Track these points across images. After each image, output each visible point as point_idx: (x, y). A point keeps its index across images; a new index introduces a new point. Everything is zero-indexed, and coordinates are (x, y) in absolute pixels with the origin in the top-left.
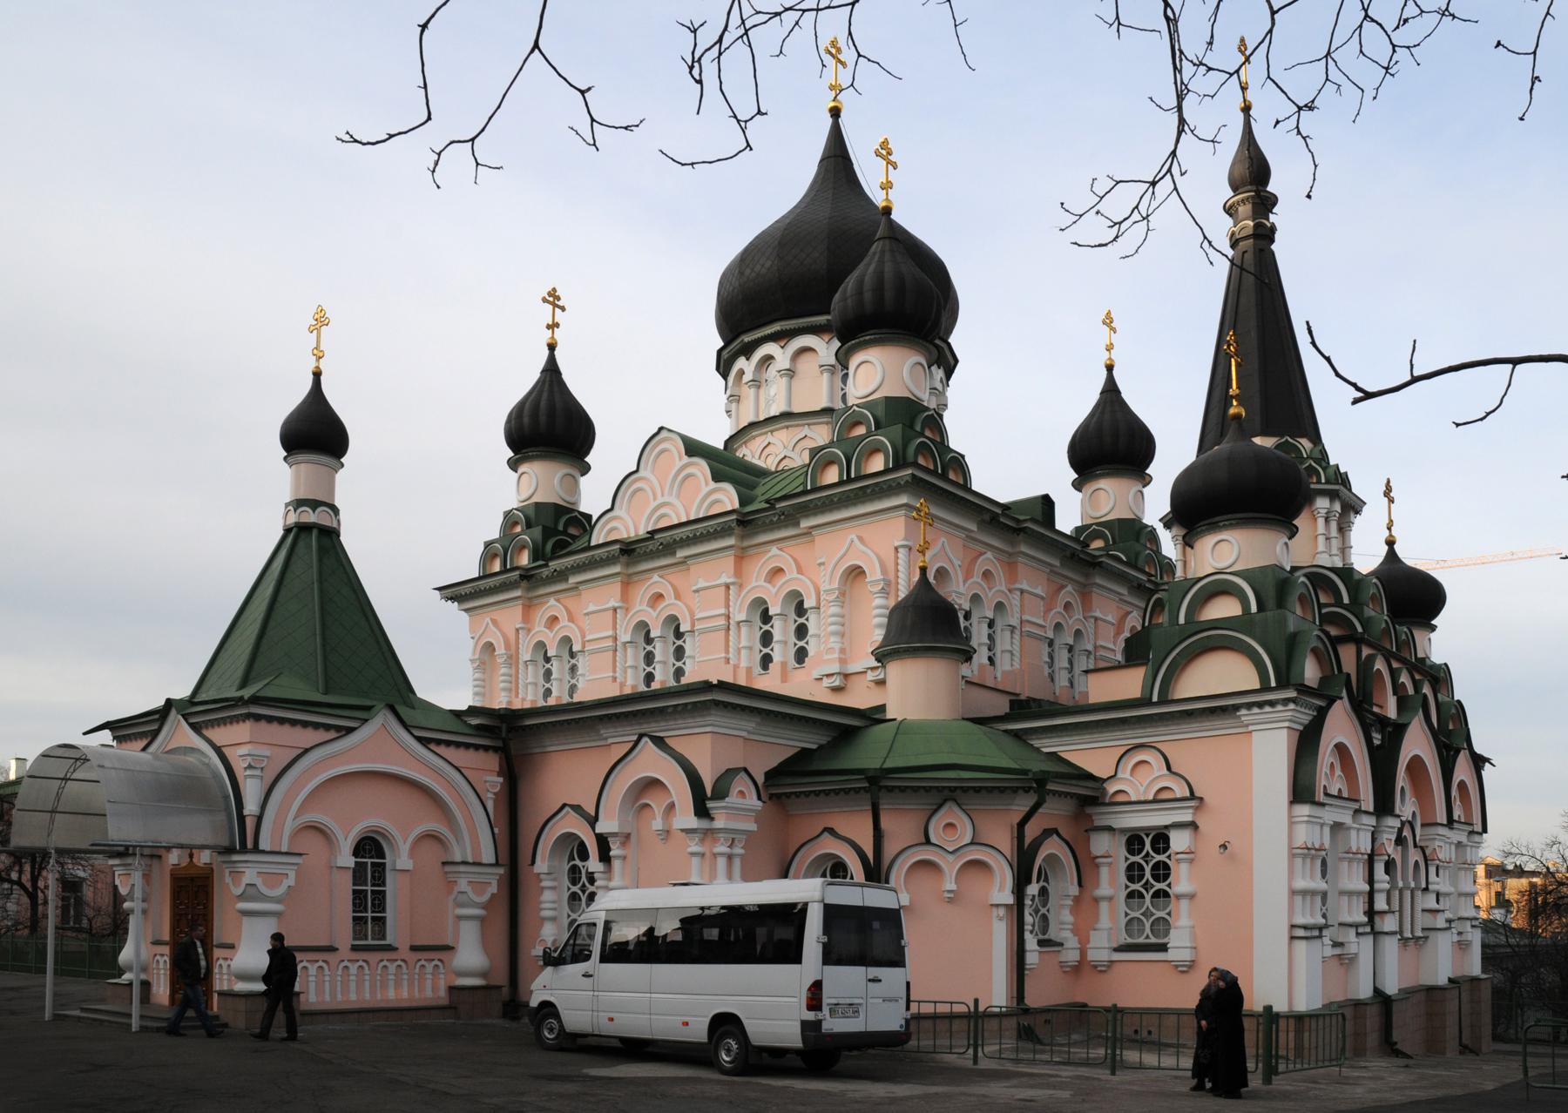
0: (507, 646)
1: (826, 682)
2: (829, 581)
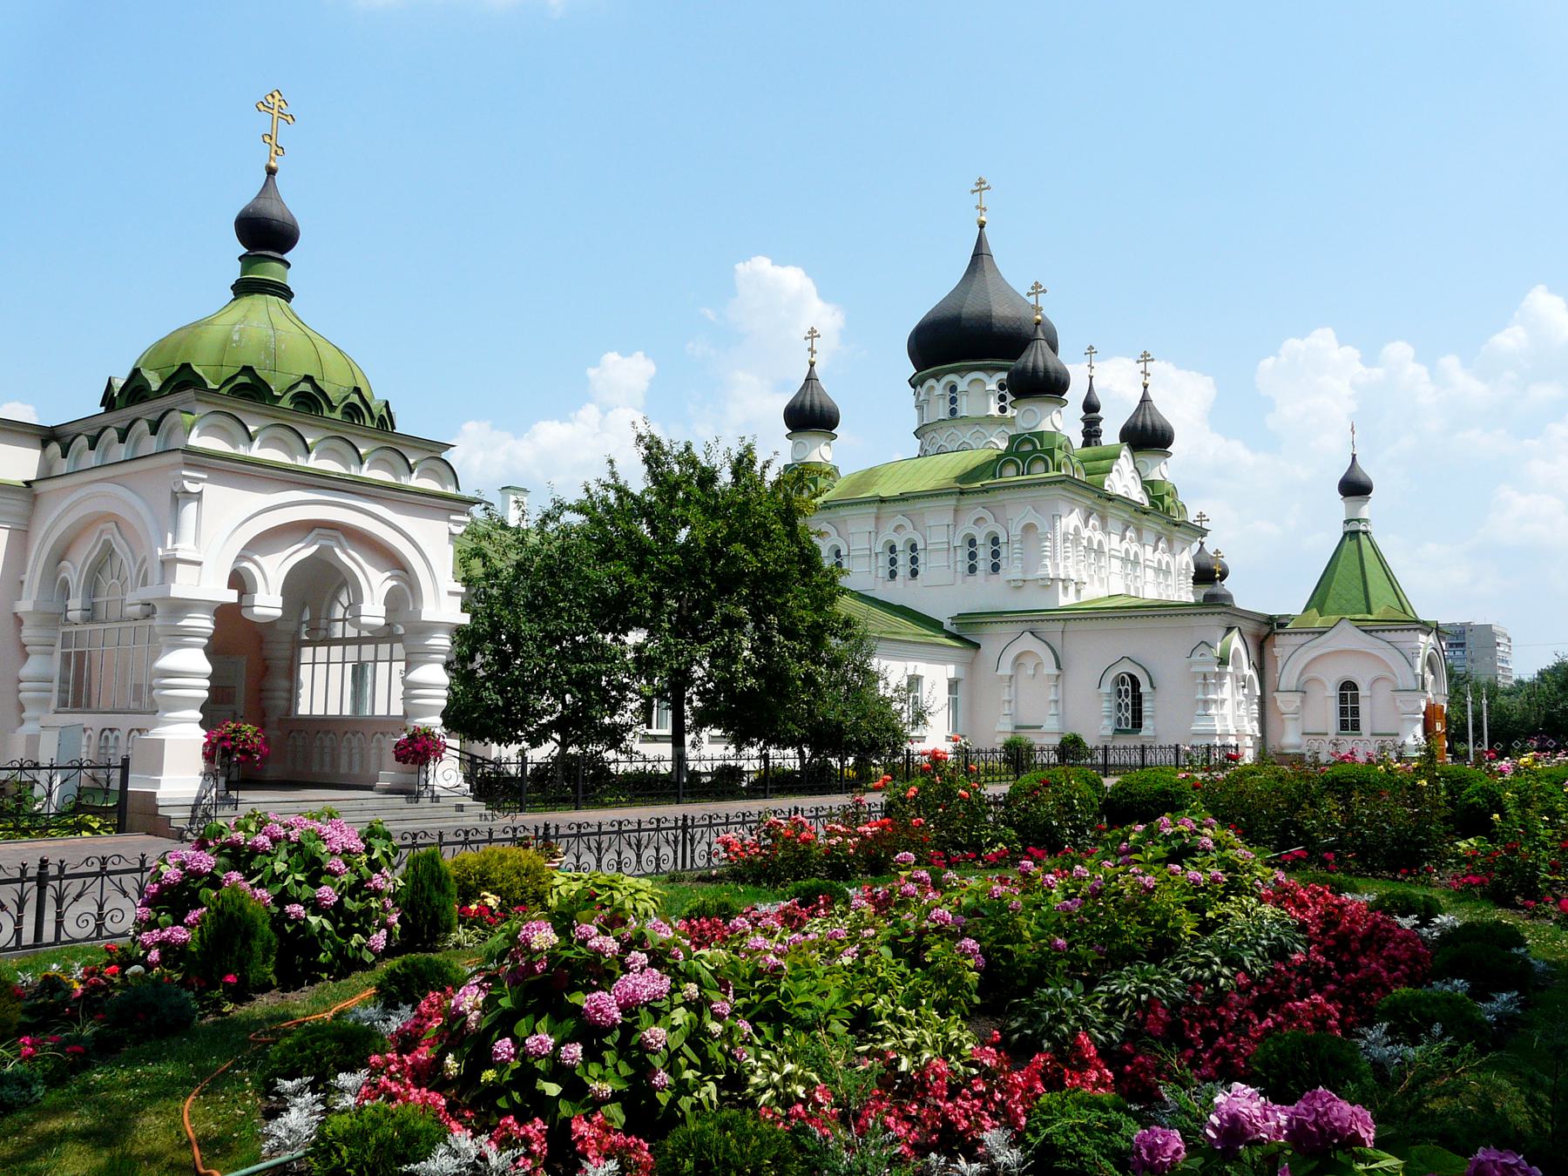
1: (1013, 584)
2: (1016, 531)
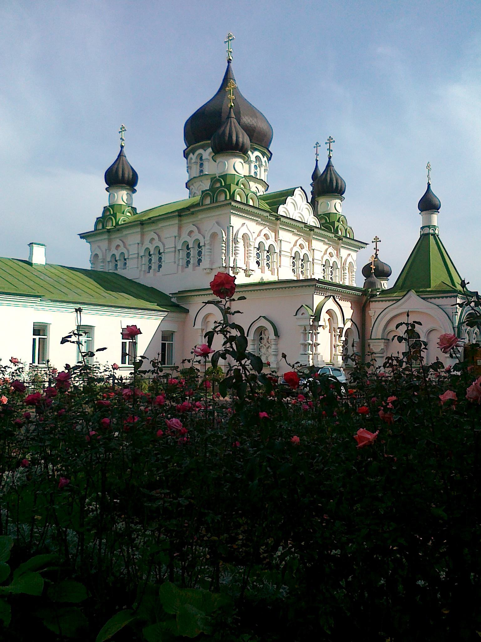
0: (103, 256)
1: (205, 271)
2: (208, 238)
